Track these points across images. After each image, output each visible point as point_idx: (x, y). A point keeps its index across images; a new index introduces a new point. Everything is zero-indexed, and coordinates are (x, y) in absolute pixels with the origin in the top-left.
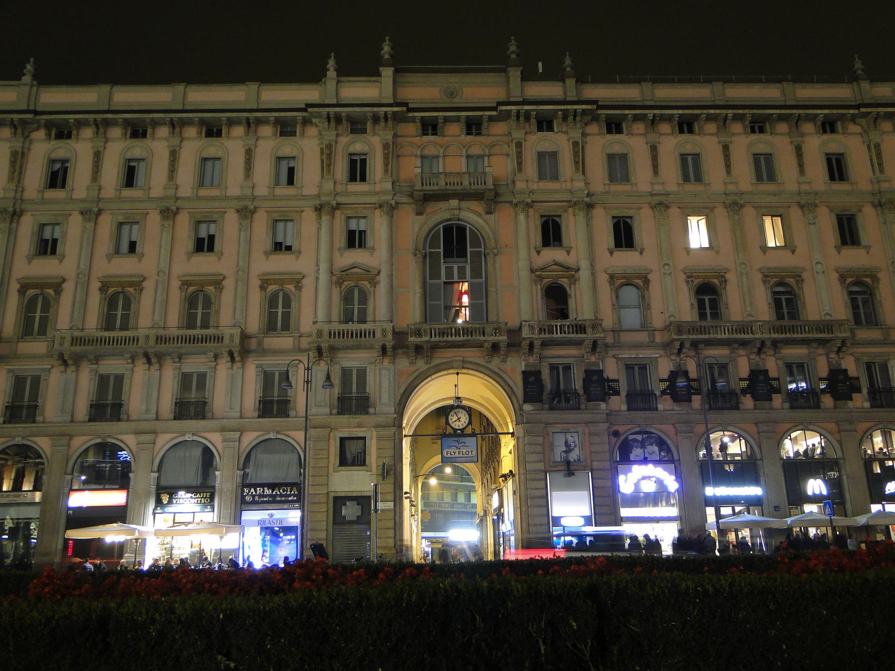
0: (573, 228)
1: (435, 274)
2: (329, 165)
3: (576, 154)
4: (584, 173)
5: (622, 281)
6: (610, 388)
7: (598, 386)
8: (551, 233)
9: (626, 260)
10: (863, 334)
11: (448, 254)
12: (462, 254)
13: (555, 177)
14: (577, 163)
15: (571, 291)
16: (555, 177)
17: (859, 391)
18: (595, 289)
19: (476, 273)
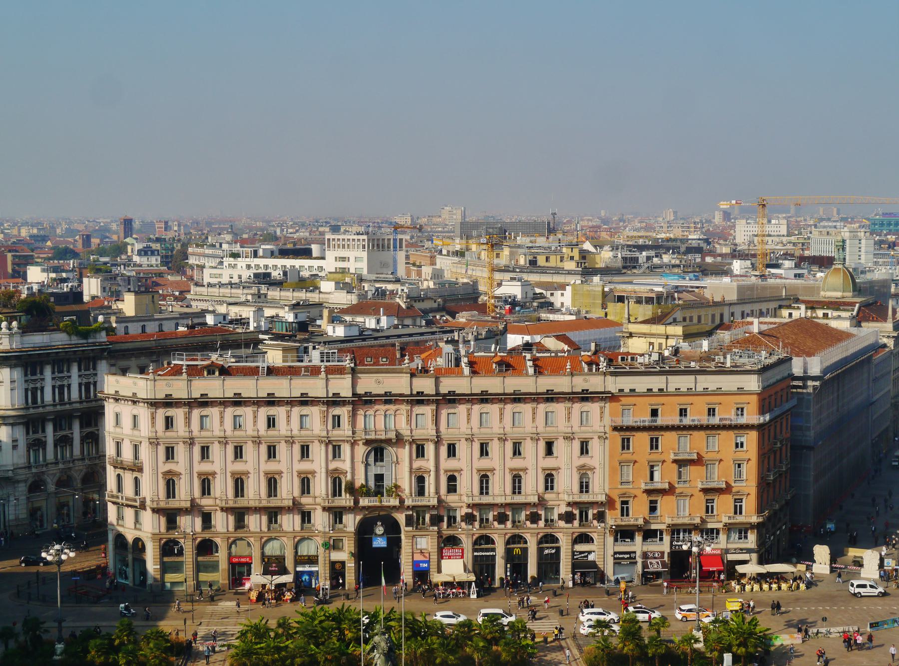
7: (436, 520)
8: (420, 452)
12: (382, 460)
15: (427, 479)
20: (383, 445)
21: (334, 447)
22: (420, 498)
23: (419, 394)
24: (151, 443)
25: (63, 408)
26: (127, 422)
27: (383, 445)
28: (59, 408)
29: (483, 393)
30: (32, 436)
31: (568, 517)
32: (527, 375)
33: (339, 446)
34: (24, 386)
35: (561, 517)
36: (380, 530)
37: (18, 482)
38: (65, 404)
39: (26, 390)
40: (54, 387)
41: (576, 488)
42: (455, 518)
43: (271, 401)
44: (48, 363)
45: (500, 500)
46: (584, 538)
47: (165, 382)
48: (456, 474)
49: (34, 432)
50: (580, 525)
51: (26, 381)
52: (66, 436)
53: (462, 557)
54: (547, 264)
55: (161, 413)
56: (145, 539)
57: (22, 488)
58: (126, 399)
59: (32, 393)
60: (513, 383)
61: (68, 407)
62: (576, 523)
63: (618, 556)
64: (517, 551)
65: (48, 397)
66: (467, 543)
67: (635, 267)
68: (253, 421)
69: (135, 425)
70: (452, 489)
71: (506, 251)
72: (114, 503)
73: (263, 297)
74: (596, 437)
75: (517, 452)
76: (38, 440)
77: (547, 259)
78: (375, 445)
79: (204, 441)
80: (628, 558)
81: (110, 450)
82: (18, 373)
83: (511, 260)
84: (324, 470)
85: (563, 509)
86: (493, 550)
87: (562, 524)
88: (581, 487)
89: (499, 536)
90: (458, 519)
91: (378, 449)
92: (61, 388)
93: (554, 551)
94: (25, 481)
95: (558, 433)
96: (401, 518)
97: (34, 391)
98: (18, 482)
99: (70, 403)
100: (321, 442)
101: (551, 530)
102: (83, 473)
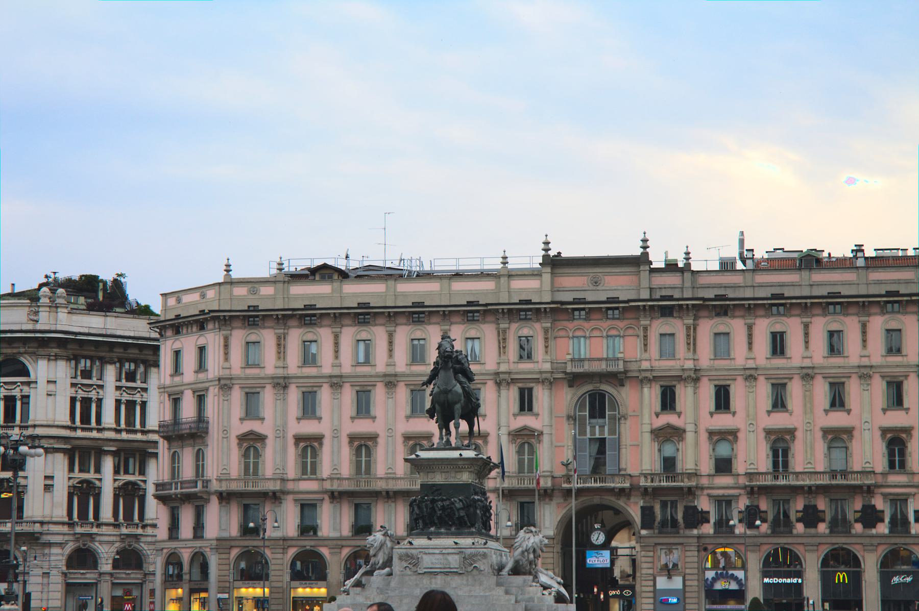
0: (684, 395)
1: (582, 432)
2: (504, 348)
3: (688, 336)
4: (695, 350)
5: (720, 436)
6: (703, 517)
7: (696, 518)
8: (668, 402)
9: (723, 421)
10: (893, 479)
11: (592, 416)
13: (673, 356)
14: (688, 344)
16: (673, 356)
17: (882, 521)
18: (697, 444)
19: (612, 431)
20: (605, 387)
25: (132, 437)
26: (189, 361)
27: (605, 387)
28: (124, 436)
30: (78, 475)
33: (530, 390)
34: (70, 392)
36: (598, 538)
37: (50, 545)
38: (136, 432)
39: (73, 400)
40: (118, 402)
44: (112, 362)
49: (81, 471)
51: (73, 385)
52: (134, 484)
57: (58, 557)
59: (85, 409)
61: (139, 436)
64: (841, 577)
65: (108, 418)
69: (201, 366)
70: (723, 466)
75: (838, 401)
76: (88, 482)
82: (62, 371)
91: (596, 394)
92: (131, 405)
94: (61, 545)
95: (909, 366)
97: (86, 402)
98: (50, 545)
99: (144, 432)
100: (498, 384)
101: (902, 540)
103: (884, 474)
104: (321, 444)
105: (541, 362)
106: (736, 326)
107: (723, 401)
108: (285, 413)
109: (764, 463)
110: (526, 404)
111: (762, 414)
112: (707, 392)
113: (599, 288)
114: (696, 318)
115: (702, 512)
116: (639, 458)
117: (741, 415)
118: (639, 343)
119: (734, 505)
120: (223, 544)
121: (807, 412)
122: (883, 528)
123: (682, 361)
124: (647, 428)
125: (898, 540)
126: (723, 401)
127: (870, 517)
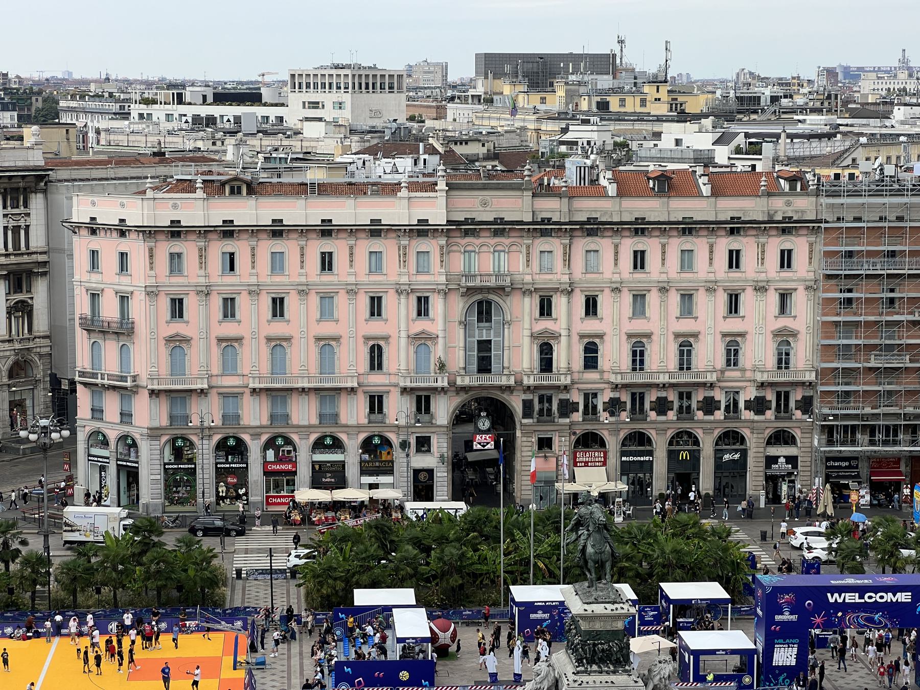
0: (560, 304)
7: (567, 408)
8: (545, 309)
10: (730, 374)
12: (489, 320)
13: (550, 271)
14: (565, 261)
15: (555, 348)
16: (550, 271)
17: (719, 409)
18: (569, 346)
20: (492, 297)
21: (419, 299)
22: (545, 375)
23: (544, 221)
24: (148, 294)
26: (109, 262)
27: (492, 297)
29: (638, 221)
31: (758, 406)
32: (700, 195)
33: (427, 299)
35: (749, 405)
41: (771, 362)
42: (595, 407)
43: (327, 230)
45: (664, 379)
46: (781, 437)
47: (171, 202)
48: (597, 341)
50: (776, 418)
53: (604, 464)
54: (622, 110)
55: (165, 248)
56: (137, 437)
58: (108, 228)
60: (680, 208)
62: (770, 414)
63: (832, 463)
64: (684, 455)
66: (613, 444)
67: (755, 112)
68: (300, 263)
70: (591, 362)
71: (561, 92)
72: (85, 384)
73: (219, 143)
74: (801, 288)
77: (622, 102)
78: (479, 297)
79: (227, 291)
80: (846, 467)
81: (82, 306)
83: (567, 104)
84: (403, 334)
85: (750, 393)
86: (650, 453)
87: (747, 415)
88: (780, 361)
89: (660, 430)
90: (600, 407)
93: (737, 456)
95: (747, 281)
96: (516, 403)
101: (734, 425)
102: (10, 362)
103: (722, 372)
104: (241, 345)
105: (437, 276)
106: (604, 245)
107: (591, 306)
108: (208, 318)
109: (626, 362)
110: (422, 307)
111: (625, 320)
112: (579, 302)
113: (487, 209)
114: (572, 237)
115: (573, 403)
116: (518, 358)
117: (607, 320)
118: (522, 258)
119: (599, 396)
120: (154, 433)
121: (662, 321)
122: (719, 415)
123: (559, 276)
124: (527, 333)
125: (730, 425)
126: (591, 306)
127: (709, 406)
